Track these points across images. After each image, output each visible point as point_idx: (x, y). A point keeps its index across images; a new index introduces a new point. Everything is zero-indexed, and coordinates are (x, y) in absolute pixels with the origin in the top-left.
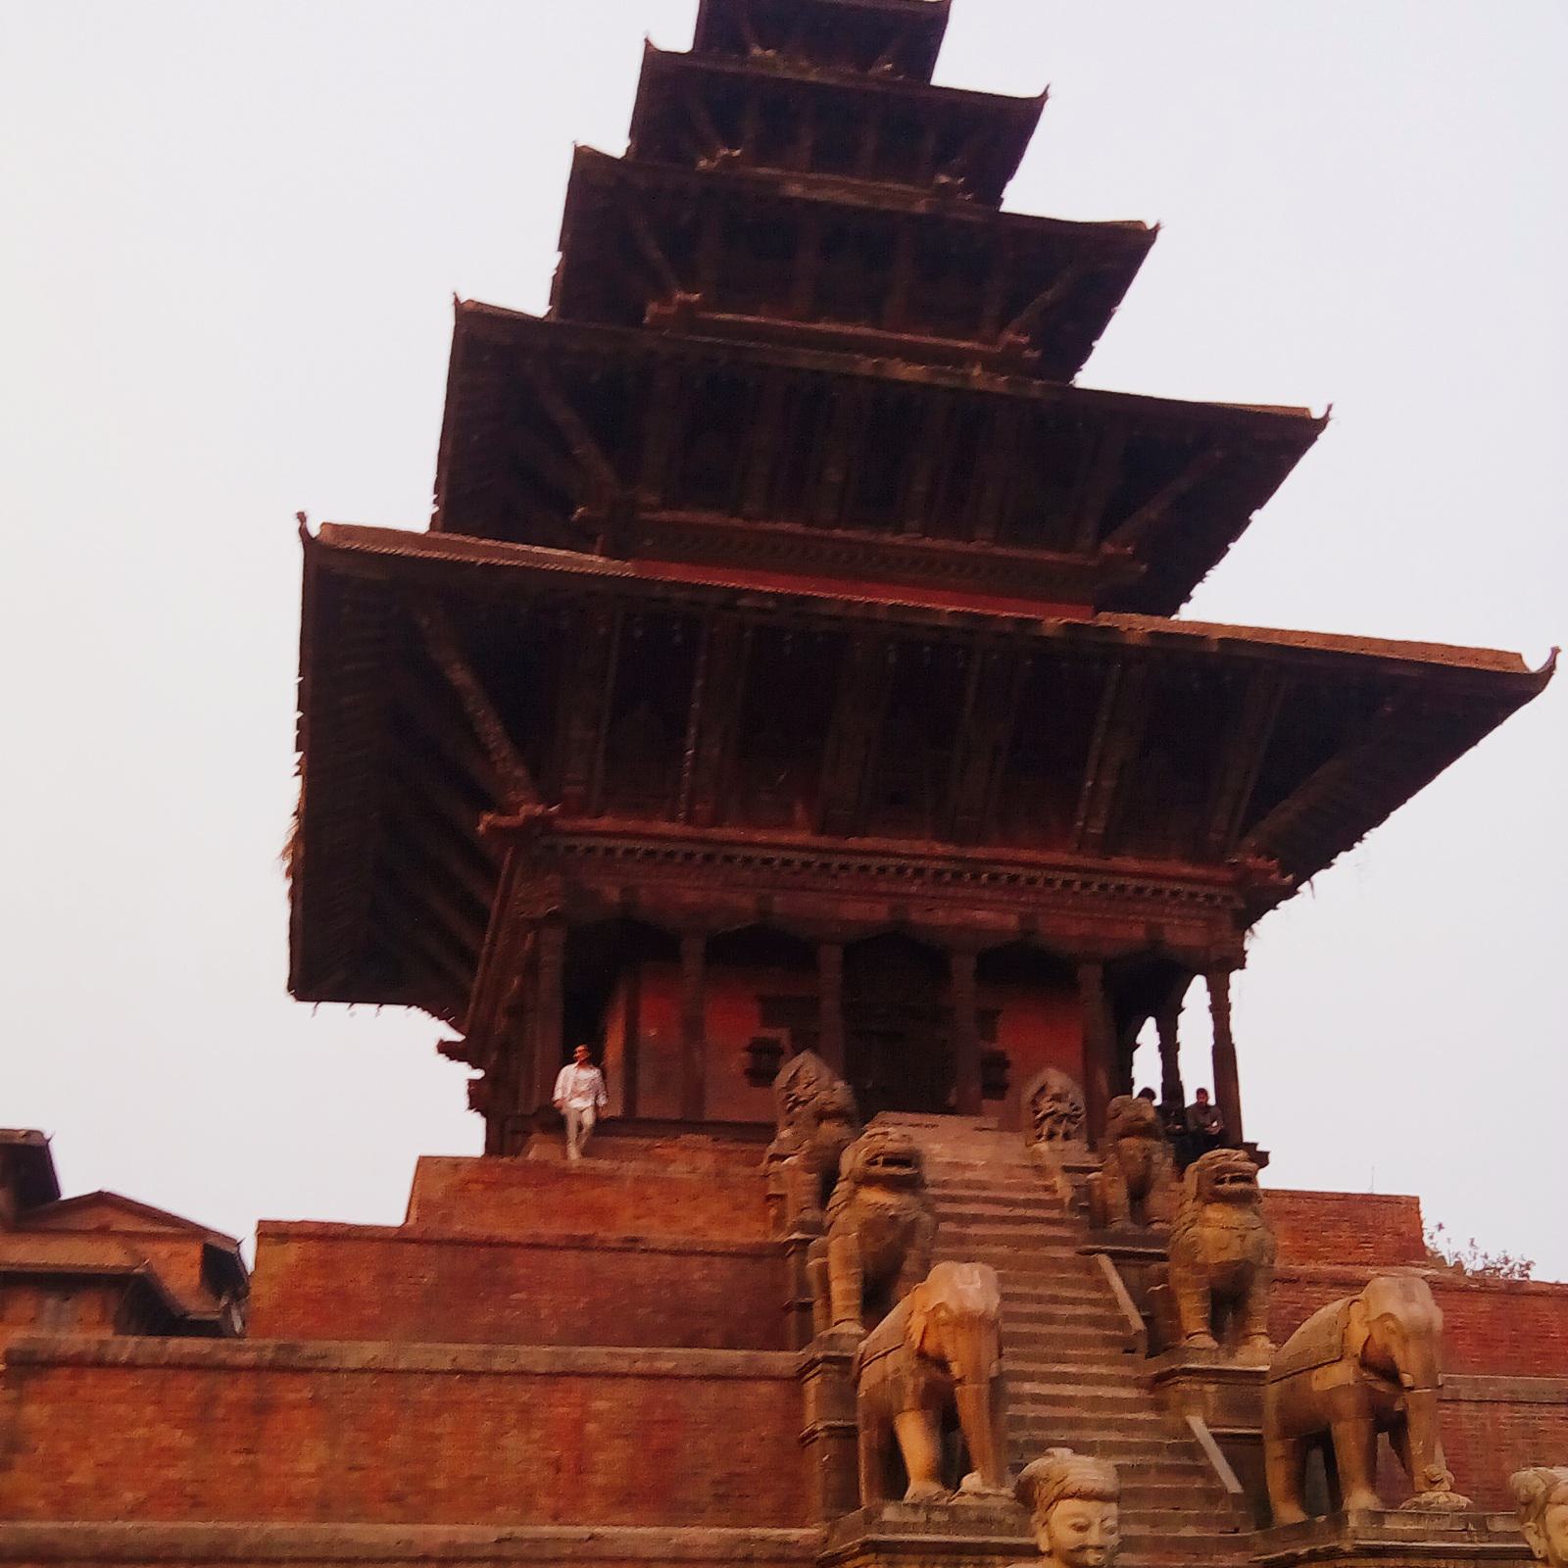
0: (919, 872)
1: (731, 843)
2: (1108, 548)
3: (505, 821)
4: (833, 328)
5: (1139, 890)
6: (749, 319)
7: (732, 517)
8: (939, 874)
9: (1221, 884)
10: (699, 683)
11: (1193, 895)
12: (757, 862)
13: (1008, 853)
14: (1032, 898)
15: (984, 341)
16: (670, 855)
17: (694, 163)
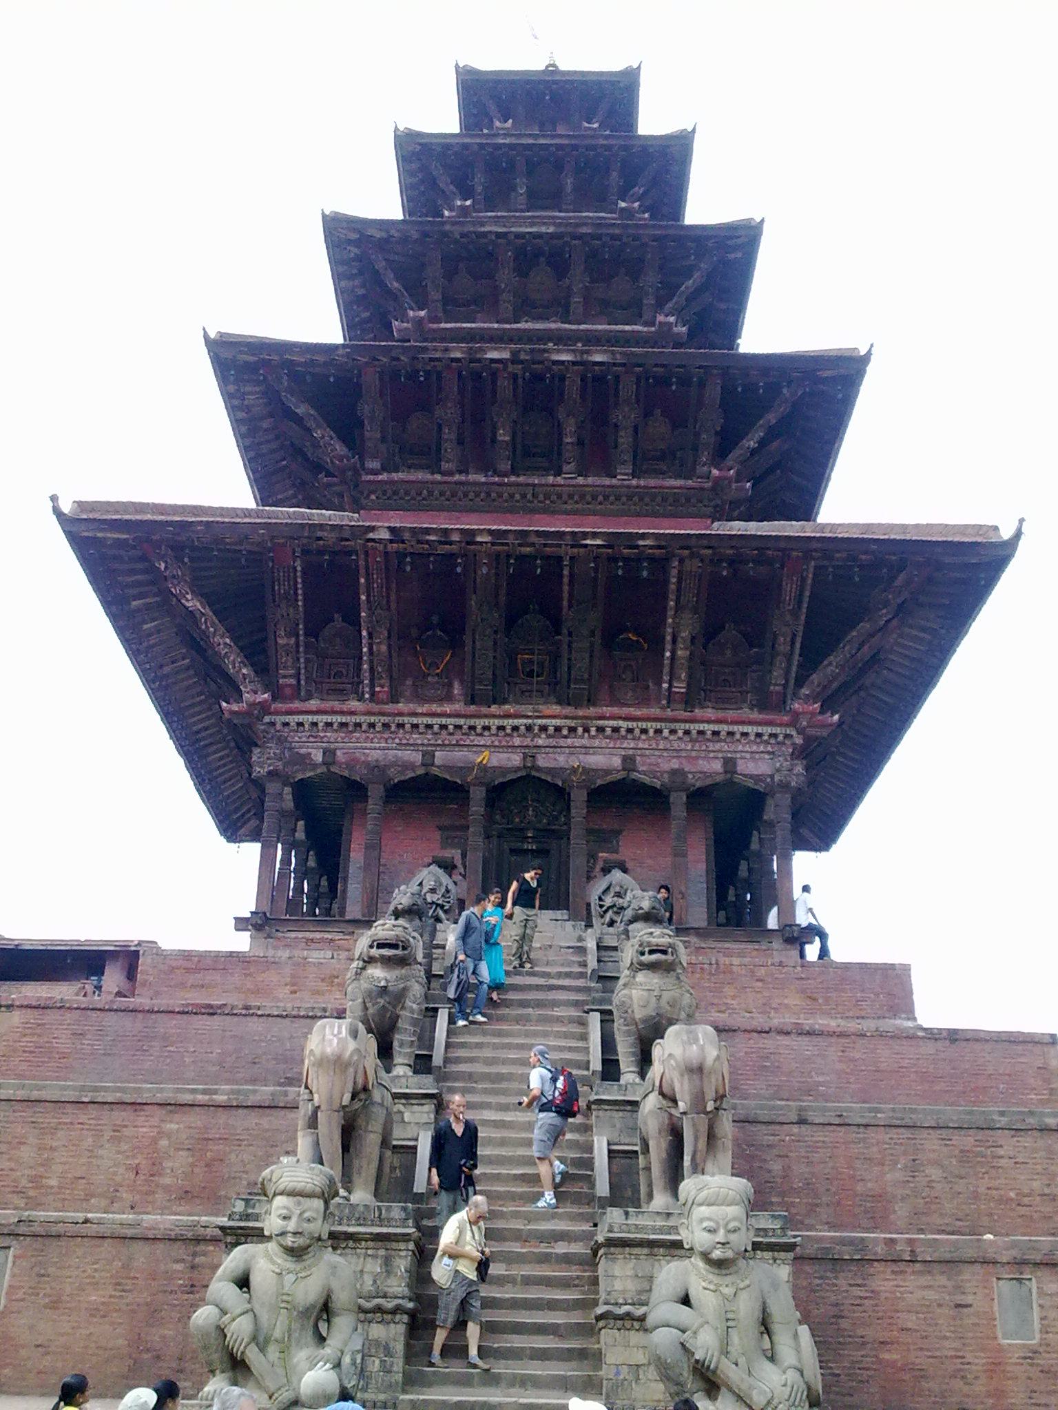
0: (544, 729)
1: (401, 714)
2: (715, 472)
3: (235, 707)
4: (529, 325)
5: (716, 733)
6: (464, 325)
7: (433, 474)
8: (558, 729)
9: (780, 725)
10: (363, 597)
11: (758, 735)
12: (422, 729)
13: (616, 710)
14: (632, 745)
15: (646, 324)
16: (358, 725)
17: (442, 216)
